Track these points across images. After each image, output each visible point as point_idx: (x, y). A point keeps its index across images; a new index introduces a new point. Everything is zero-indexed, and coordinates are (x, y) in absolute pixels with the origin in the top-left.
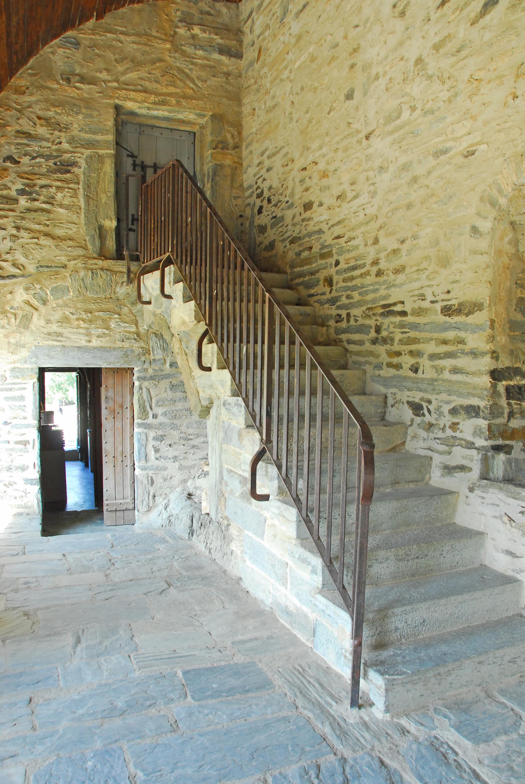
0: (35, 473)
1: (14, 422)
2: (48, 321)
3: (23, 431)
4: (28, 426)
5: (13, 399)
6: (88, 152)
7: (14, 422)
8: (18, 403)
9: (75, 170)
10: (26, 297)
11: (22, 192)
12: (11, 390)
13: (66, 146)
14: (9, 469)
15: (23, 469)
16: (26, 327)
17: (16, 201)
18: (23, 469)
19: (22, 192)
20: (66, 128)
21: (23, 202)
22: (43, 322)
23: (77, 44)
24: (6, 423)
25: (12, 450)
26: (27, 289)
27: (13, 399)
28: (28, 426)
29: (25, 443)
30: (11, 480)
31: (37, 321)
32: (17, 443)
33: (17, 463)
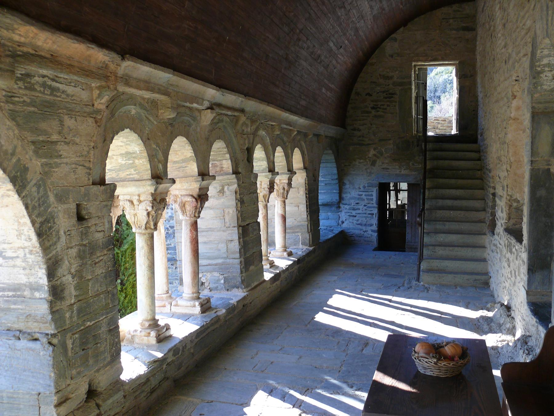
0: (375, 227)
1: (369, 205)
2: (383, 163)
3: (372, 209)
4: (374, 207)
5: (368, 195)
6: (400, 88)
7: (369, 205)
8: (370, 197)
9: (395, 96)
10: (374, 152)
11: (373, 108)
12: (367, 192)
13: (391, 86)
14: (365, 225)
15: (371, 225)
16: (374, 166)
17: (371, 112)
18: (371, 225)
19: (373, 108)
20: (392, 78)
21: (373, 112)
22: (381, 164)
23: (395, 40)
24: (365, 206)
25: (367, 217)
26: (375, 149)
27: (368, 195)
28: (374, 207)
29: (372, 214)
30: (366, 229)
31: (378, 163)
32: (369, 214)
33: (368, 223)
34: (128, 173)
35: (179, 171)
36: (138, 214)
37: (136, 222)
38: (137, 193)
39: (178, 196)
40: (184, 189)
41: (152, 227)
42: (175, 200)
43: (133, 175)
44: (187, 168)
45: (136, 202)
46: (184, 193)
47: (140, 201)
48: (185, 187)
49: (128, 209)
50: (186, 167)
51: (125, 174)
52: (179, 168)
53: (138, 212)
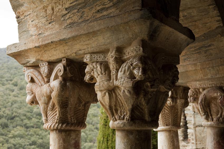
34: (98, 8)
35: (199, 53)
36: (118, 91)
37: (114, 107)
38: (115, 45)
39: (199, 90)
40: (208, 79)
41: (147, 118)
42: (195, 96)
43: (107, 9)
44: (212, 47)
45: (112, 65)
46: (207, 84)
47: (120, 61)
48: (209, 76)
49: (98, 80)
50: (210, 46)
51: (94, 11)
52: (199, 49)
53: (116, 83)
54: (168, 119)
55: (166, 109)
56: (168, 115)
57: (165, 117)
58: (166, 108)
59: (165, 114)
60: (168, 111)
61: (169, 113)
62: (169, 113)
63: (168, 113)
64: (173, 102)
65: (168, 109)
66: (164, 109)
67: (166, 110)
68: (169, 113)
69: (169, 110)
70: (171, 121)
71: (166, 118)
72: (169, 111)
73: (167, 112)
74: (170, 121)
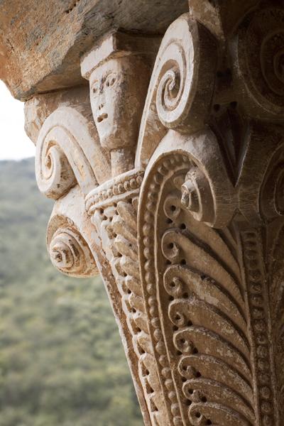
54: (220, 375)
55: (194, 270)
56: (222, 339)
57: (194, 351)
58: (197, 257)
59: (194, 316)
60: (222, 289)
61: (227, 307)
62: (236, 316)
63: (219, 311)
64: (233, 178)
65: (217, 272)
66: (183, 263)
67: (196, 283)
68: (236, 316)
69: (227, 282)
70: (261, 401)
71: (205, 362)
72: (222, 289)
73: (214, 301)
74: (253, 400)
